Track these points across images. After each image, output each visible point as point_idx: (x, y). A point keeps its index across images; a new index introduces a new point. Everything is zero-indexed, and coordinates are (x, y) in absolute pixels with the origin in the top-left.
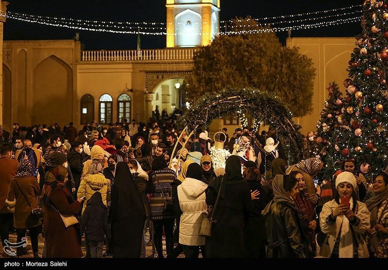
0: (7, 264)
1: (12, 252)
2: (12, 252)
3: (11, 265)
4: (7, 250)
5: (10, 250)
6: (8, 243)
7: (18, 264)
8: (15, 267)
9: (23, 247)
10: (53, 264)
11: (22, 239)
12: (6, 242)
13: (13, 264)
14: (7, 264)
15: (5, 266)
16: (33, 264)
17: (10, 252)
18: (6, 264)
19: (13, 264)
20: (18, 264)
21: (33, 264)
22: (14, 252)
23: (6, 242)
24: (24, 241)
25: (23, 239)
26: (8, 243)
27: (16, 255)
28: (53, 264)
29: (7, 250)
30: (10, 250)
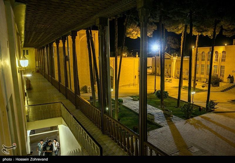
0: (4, 160)
1: (7, 152)
2: (7, 152)
3: (7, 160)
4: (4, 151)
5: (6, 151)
6: (5, 147)
7: (11, 160)
8: (9, 162)
9: (14, 149)
10: (32, 159)
11: (13, 145)
12: (3, 146)
13: (8, 160)
14: (4, 160)
15: (3, 160)
16: (19, 160)
17: (6, 153)
18: (4, 160)
19: (8, 160)
20: (11, 160)
21: (19, 160)
22: (8, 152)
23: (3, 146)
24: (14, 145)
25: (14, 144)
26: (5, 147)
27: (9, 154)
28: (32, 159)
29: (4, 151)
30: (6, 151)
